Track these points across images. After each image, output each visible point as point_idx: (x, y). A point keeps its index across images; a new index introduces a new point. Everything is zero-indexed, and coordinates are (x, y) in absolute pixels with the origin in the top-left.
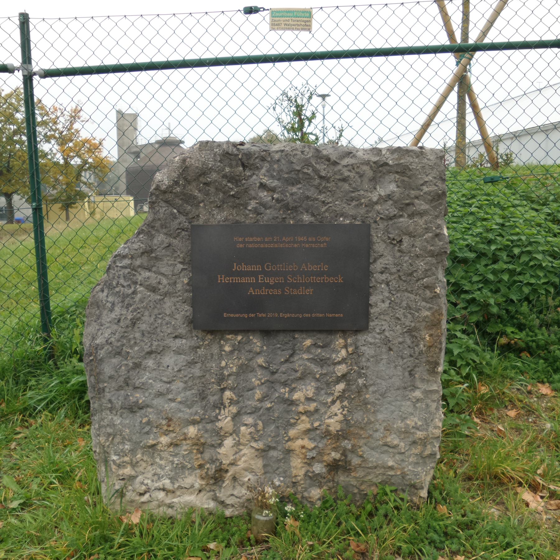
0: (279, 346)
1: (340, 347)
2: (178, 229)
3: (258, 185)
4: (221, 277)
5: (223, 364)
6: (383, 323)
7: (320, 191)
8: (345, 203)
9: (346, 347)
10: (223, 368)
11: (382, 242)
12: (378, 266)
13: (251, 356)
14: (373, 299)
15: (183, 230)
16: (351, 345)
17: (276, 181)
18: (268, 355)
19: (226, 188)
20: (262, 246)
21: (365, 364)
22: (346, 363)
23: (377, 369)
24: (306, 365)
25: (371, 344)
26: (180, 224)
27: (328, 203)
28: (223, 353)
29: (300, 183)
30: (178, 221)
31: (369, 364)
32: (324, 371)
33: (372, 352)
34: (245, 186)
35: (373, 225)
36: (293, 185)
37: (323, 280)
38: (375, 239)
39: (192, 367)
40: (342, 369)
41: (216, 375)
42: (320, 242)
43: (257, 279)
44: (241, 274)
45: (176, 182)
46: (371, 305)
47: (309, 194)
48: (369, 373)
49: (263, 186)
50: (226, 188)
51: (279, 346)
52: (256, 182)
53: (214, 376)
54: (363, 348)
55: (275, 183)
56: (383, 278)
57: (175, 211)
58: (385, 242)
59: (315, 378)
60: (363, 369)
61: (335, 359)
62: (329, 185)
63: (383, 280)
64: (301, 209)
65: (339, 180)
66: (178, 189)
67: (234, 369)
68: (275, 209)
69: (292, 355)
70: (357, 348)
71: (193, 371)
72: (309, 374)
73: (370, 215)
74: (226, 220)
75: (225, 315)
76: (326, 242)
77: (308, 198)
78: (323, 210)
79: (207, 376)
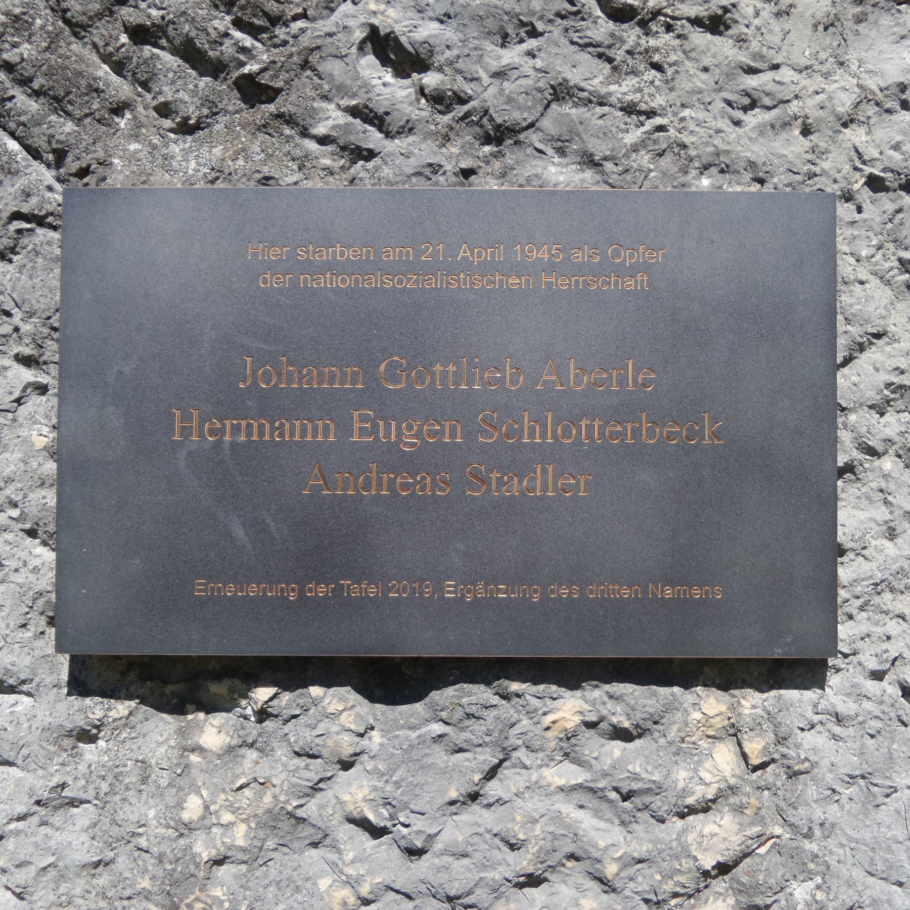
0: (437, 728)
1: (704, 734)
2: (17, 216)
3: (359, 35)
4: (186, 417)
5: (193, 808)
6: (893, 627)
7: (615, 69)
8: (723, 114)
9: (734, 733)
10: (186, 829)
11: (874, 282)
12: (859, 380)
13: (314, 770)
14: (853, 517)
15: (40, 221)
16: (756, 726)
17: (435, 25)
18: (392, 771)
19: (227, 48)
20: (372, 283)
21: (818, 814)
22: (739, 810)
23: (866, 835)
24: (558, 818)
25: (839, 719)
26: (27, 195)
27: (651, 114)
28: (194, 758)
29: (534, 33)
30: (21, 183)
31: (833, 812)
32: (640, 849)
33: (849, 762)
34: (305, 41)
35: (845, 211)
36: (505, 40)
37: (636, 433)
38: (846, 267)
39: (57, 819)
40: (717, 835)
41: (161, 859)
42: (621, 272)
43: (345, 429)
44: (270, 406)
45: (17, 18)
46: (842, 552)
47: (574, 77)
48: (835, 850)
49: (382, 44)
50: (227, 48)
51: (437, 728)
52: (351, 23)
53: (151, 862)
54: (809, 739)
55: (428, 30)
56: (890, 432)
57: (13, 145)
58: (888, 283)
59: (601, 880)
60: (809, 836)
61: (685, 793)
62: (652, 42)
63: (889, 441)
64: (534, 137)
65: (696, 22)
66: (26, 49)
67: (240, 836)
68: (428, 135)
69: (492, 773)
70: (781, 740)
71: (58, 838)
72: (572, 857)
73: (826, 165)
74: (218, 173)
75: (200, 588)
76: (646, 268)
77: (561, 92)
78: (633, 136)
79: (122, 863)
